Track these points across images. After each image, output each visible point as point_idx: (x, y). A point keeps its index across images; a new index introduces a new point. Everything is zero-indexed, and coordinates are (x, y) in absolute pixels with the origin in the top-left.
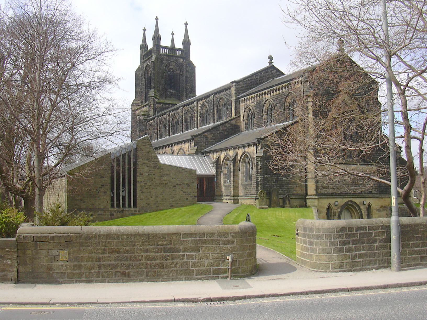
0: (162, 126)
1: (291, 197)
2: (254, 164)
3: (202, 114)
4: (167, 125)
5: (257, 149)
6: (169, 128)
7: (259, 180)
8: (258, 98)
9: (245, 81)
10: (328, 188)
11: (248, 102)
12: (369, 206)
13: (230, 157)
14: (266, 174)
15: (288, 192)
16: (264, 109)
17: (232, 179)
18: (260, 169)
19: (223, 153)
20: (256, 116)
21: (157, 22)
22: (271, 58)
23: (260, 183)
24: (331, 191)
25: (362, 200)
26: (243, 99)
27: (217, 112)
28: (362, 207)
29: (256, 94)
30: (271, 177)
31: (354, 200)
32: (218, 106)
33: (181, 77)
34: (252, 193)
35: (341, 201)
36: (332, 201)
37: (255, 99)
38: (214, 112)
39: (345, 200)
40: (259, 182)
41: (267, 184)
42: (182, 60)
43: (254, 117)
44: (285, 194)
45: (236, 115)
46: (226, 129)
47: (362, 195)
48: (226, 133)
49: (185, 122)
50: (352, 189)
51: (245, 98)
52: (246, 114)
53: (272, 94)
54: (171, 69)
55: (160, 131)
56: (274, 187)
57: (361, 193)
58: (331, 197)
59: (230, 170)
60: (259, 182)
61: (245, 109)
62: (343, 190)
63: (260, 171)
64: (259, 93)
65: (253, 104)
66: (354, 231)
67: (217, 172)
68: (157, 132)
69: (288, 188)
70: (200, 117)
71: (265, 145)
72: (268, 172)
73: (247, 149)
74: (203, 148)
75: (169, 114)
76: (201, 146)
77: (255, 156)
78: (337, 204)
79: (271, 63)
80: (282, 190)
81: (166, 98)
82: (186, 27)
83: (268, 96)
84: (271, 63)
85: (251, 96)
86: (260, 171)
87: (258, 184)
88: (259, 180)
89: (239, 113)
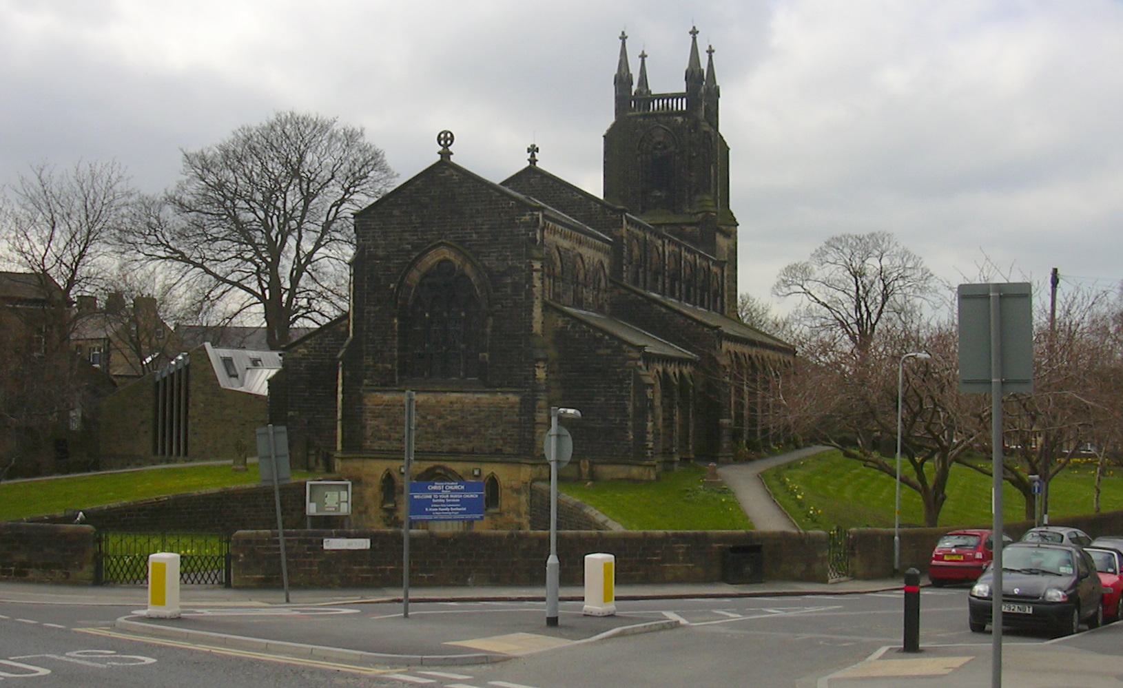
10: (389, 439)
21: (624, 44)
22: (533, 150)
25: (470, 466)
31: (449, 465)
33: (677, 158)
42: (680, 119)
47: (473, 455)
50: (448, 442)
54: (659, 143)
57: (472, 452)
79: (533, 161)
82: (694, 39)
84: (533, 161)
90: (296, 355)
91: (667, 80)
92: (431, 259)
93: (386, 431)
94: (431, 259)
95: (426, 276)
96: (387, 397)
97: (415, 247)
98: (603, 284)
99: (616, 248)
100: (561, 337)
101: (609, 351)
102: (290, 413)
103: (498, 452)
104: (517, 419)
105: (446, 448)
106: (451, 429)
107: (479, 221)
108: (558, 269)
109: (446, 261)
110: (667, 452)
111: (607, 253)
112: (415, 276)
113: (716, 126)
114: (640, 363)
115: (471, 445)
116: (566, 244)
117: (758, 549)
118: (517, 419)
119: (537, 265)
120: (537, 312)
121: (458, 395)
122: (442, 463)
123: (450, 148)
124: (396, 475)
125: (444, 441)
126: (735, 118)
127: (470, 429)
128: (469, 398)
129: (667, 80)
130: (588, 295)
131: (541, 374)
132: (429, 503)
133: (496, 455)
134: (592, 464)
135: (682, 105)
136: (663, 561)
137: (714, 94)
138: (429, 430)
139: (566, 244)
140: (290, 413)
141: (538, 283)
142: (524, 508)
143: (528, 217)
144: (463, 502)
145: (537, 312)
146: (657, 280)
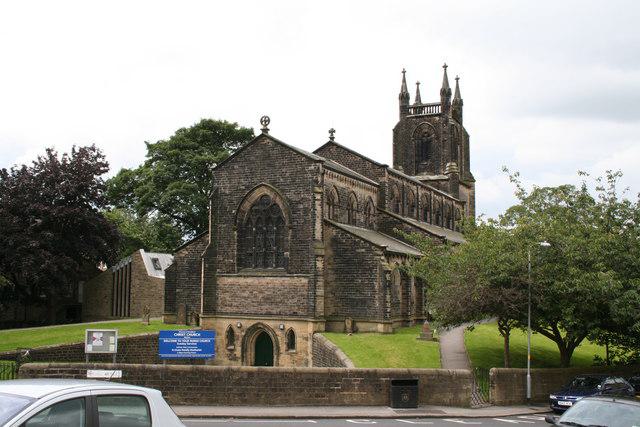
22: (332, 132)
24: (235, 309)
25: (278, 323)
28: (278, 333)
36: (235, 323)
39: (255, 322)
42: (437, 118)
50: (265, 308)
57: (279, 314)
62: (252, 309)
66: (307, 364)
79: (332, 138)
90: (181, 255)
91: (431, 96)
92: (257, 194)
94: (257, 194)
95: (254, 205)
96: (230, 280)
97: (247, 187)
98: (372, 212)
99: (380, 189)
100: (335, 241)
101: (363, 250)
103: (295, 314)
104: (305, 293)
105: (264, 312)
106: (267, 299)
107: (284, 170)
108: (336, 200)
109: (266, 195)
110: (405, 315)
111: (375, 192)
112: (247, 205)
113: (461, 124)
114: (383, 258)
116: (342, 185)
117: (415, 382)
118: (305, 293)
119: (318, 197)
120: (318, 226)
123: (268, 127)
124: (235, 329)
126: (472, 121)
128: (278, 281)
129: (431, 96)
130: (361, 217)
131: (320, 265)
132: (174, 345)
134: (353, 323)
135: (439, 110)
136: (343, 390)
137: (459, 103)
139: (342, 185)
141: (318, 208)
142: (310, 350)
143: (313, 167)
144: (199, 345)
145: (318, 226)
146: (413, 211)
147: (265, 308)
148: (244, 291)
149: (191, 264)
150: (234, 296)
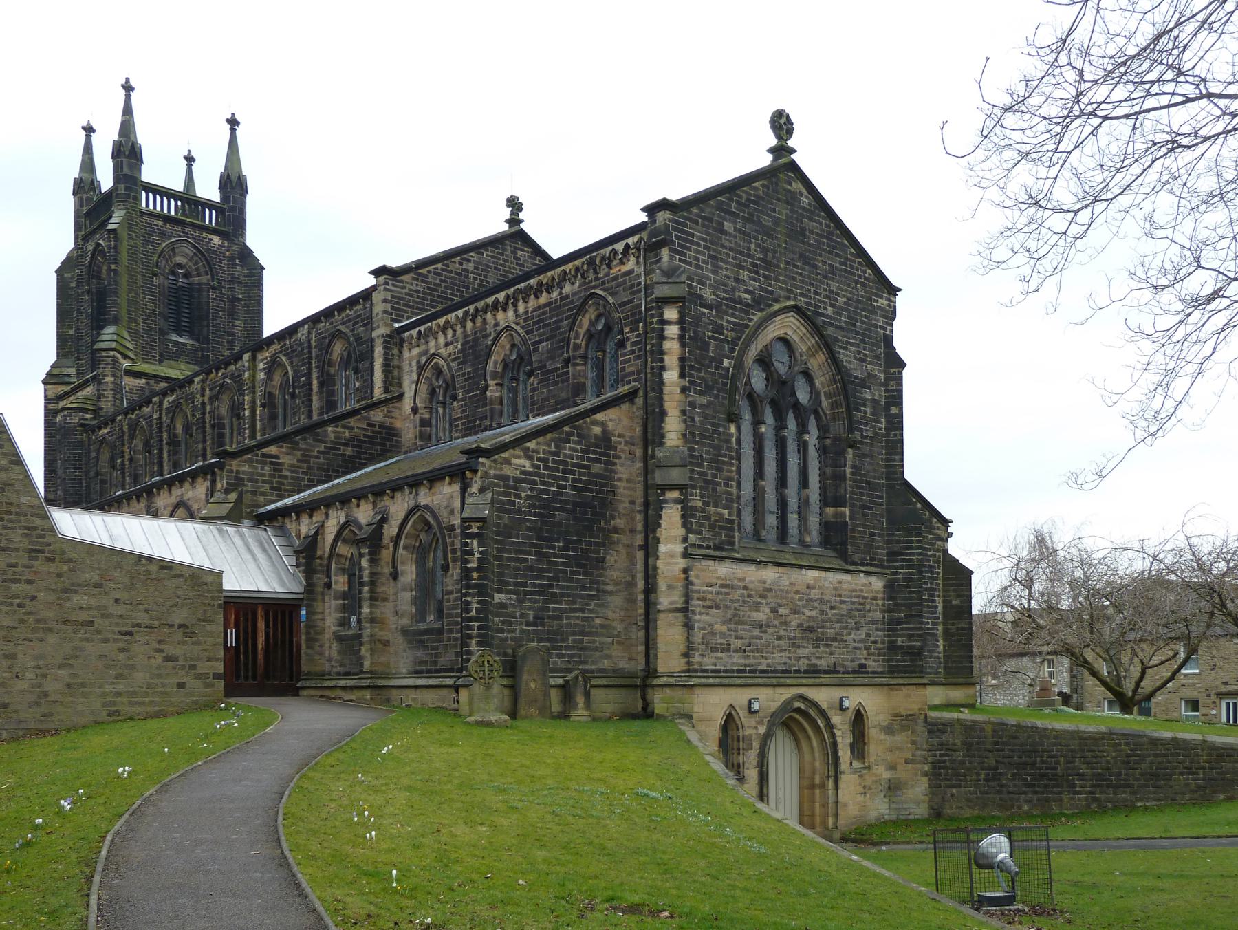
0: (138, 443)
1: (594, 682)
2: (454, 551)
3: (270, 394)
4: (154, 441)
5: (464, 490)
6: (161, 450)
7: (473, 613)
8: (469, 325)
9: (424, 271)
10: (727, 649)
11: (432, 343)
12: (859, 718)
13: (360, 527)
14: (500, 591)
15: (581, 662)
16: (490, 367)
17: (366, 610)
18: (478, 569)
19: (333, 513)
20: (461, 394)
23: (476, 624)
24: (737, 660)
26: (414, 332)
27: (321, 384)
29: (460, 313)
30: (520, 601)
32: (325, 363)
34: (443, 662)
35: (770, 699)
36: (739, 697)
37: (459, 331)
38: (310, 384)
40: (471, 619)
41: (502, 631)
42: (217, 240)
43: (454, 398)
44: (570, 671)
45: (386, 390)
46: (351, 439)
48: (349, 451)
49: (213, 427)
51: (422, 328)
52: (424, 388)
53: (521, 308)
54: (180, 266)
55: (131, 460)
56: (529, 640)
58: (738, 681)
59: (361, 577)
60: (471, 619)
61: (421, 369)
62: (777, 659)
63: (475, 575)
64: (472, 308)
65: (450, 349)
67: (310, 588)
68: (123, 464)
69: (582, 649)
70: (263, 406)
71: (496, 477)
72: (507, 583)
73: (424, 497)
74: (261, 499)
75: (161, 402)
76: (254, 493)
77: (457, 521)
78: (756, 706)
80: (560, 656)
81: (160, 362)
83: (506, 318)
84: (514, 221)
85: (442, 321)
86: (475, 575)
87: (471, 628)
88: (473, 613)
89: (400, 385)
90: (507, 470)
93: (723, 635)
102: (498, 598)
104: (879, 615)
115: (832, 659)
118: (879, 615)
121: (815, 574)
122: (802, 691)
125: (801, 652)
127: (831, 633)
133: (858, 675)
138: (782, 633)
140: (498, 598)
147: (806, 652)
148: (757, 607)
149: (543, 506)
150: (735, 620)
